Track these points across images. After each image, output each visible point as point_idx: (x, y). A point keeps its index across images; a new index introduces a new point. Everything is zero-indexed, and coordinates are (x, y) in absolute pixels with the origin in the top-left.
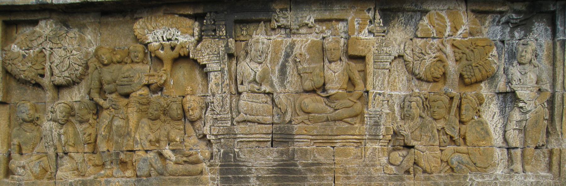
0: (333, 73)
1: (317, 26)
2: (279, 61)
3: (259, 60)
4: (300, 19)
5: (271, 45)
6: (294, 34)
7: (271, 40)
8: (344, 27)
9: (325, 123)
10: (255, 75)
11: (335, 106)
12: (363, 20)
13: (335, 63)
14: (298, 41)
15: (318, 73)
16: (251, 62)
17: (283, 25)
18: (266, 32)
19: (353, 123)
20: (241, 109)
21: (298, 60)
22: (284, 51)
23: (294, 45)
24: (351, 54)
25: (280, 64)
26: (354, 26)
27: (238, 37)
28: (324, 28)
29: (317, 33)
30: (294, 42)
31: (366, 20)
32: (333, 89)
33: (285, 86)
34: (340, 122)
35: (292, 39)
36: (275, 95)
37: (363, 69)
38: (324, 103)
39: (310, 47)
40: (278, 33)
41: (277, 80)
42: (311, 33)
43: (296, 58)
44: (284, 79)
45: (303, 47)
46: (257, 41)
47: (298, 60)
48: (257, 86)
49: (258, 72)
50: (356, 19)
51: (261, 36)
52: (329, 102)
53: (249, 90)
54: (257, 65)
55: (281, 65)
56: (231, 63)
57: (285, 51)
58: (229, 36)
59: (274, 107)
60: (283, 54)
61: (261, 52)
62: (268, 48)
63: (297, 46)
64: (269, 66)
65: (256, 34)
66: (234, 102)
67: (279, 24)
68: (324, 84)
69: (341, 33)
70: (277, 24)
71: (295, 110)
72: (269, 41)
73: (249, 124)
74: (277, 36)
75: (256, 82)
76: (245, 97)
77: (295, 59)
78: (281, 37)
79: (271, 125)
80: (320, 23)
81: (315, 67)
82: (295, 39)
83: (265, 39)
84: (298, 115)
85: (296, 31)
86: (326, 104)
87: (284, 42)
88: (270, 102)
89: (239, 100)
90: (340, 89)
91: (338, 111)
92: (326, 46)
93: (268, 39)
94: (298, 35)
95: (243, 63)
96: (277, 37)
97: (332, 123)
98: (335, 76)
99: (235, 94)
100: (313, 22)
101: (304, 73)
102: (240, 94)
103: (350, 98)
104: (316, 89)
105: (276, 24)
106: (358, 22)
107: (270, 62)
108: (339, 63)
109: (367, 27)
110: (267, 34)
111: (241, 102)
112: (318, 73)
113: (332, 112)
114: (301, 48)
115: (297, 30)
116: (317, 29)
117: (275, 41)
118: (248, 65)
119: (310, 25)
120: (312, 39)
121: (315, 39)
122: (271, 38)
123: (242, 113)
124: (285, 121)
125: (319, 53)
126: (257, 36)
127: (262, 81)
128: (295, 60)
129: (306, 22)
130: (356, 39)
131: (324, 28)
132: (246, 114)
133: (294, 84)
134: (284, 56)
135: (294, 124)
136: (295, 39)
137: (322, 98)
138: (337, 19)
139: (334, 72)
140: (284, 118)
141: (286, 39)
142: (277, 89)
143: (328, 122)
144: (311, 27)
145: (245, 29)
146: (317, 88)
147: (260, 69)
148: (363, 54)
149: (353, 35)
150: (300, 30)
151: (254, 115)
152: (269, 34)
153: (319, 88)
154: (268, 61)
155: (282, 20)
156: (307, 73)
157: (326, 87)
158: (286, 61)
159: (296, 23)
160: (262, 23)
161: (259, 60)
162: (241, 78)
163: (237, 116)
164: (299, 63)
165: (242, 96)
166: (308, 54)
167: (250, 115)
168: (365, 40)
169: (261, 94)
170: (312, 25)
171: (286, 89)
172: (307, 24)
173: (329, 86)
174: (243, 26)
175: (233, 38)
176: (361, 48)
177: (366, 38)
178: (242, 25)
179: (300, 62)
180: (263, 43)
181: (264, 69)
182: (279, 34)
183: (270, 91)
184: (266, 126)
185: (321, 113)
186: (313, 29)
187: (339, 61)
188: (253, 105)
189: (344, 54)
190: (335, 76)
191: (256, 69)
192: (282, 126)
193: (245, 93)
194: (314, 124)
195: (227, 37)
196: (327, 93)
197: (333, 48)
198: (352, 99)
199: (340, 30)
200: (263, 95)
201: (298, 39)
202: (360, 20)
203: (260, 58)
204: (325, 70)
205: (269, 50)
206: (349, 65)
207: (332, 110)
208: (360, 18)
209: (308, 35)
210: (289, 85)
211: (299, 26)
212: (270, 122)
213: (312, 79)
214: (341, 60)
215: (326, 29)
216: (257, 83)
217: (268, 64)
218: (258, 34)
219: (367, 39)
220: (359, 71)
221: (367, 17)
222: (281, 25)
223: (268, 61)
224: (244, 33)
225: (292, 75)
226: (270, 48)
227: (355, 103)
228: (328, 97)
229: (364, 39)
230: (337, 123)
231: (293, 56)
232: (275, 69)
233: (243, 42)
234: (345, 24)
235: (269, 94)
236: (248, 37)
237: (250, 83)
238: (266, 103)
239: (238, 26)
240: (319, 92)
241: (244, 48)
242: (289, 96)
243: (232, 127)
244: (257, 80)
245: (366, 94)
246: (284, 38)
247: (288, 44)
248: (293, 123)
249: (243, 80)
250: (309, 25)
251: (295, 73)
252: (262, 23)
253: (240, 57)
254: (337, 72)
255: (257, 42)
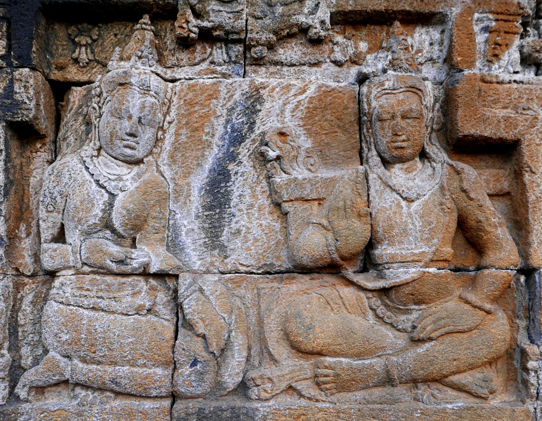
0: (404, 203)
1: (339, 38)
2: (203, 156)
3: (129, 151)
4: (280, 10)
5: (175, 99)
6: (258, 62)
7: (177, 83)
8: (431, 44)
9: (377, 392)
10: (111, 205)
11: (414, 327)
12: (501, 17)
13: (406, 166)
14: (273, 89)
15: (349, 203)
16: (101, 157)
17: (220, 27)
18: (160, 54)
19: (486, 391)
20: (50, 340)
21: (272, 154)
22: (222, 120)
23: (259, 100)
24: (466, 133)
25: (207, 166)
26: (471, 35)
27: (61, 68)
28: (363, 46)
29: (338, 64)
30: (257, 90)
31: (511, 18)
32: (404, 262)
33: (223, 248)
34: (434, 386)
35: (252, 82)
36: (185, 280)
37: (505, 185)
38: (370, 314)
39: (315, 109)
40: (204, 60)
41: (196, 225)
42: (317, 64)
43: (266, 145)
44: (221, 218)
45: (289, 107)
46: (123, 81)
47: (272, 154)
48: (114, 249)
49: (121, 196)
50: (476, 15)
51: (139, 64)
52: (386, 306)
53: (84, 264)
54: (123, 170)
55: (210, 171)
56: (29, 161)
57: (227, 121)
58: (18, 58)
59: (181, 331)
60: (220, 130)
61: (135, 118)
62: (165, 108)
63: (267, 105)
64: (168, 174)
65: (121, 59)
66: (26, 306)
67: (206, 24)
68: (371, 245)
69: (421, 64)
70: (199, 21)
71: (263, 341)
72: (171, 85)
73: (81, 392)
74: (198, 68)
75: (114, 231)
76: (69, 290)
77: (264, 148)
78: (213, 72)
79: (167, 403)
80: (349, 31)
81: (333, 181)
82: (259, 80)
83: (154, 76)
84: (275, 361)
85: (265, 52)
86: (377, 316)
87: (223, 89)
88: (166, 312)
89: (45, 300)
90: (432, 261)
91: (427, 345)
92: (374, 104)
93: (166, 80)
94: (272, 69)
95: (68, 158)
96: (199, 73)
97: (400, 391)
98: (410, 215)
99: (33, 276)
100: (328, 21)
101: (297, 199)
102: (52, 274)
103: (471, 297)
104: (342, 262)
105: (194, 21)
106: (486, 23)
107: (172, 156)
108: (419, 165)
109: (517, 42)
110: (160, 61)
111: (52, 307)
112: (349, 203)
113: (403, 350)
114: (282, 111)
115: (271, 47)
116: (337, 49)
117: (190, 87)
118: (87, 168)
119: (317, 30)
120: (320, 82)
121: (333, 84)
122: (178, 77)
123: (52, 353)
124: (218, 385)
125: (345, 130)
126: (122, 63)
127: (137, 228)
128: (262, 154)
129: (302, 19)
130: (483, 80)
131: (363, 46)
132: (68, 357)
133: (256, 240)
134: (222, 138)
135: (259, 399)
136: (261, 80)
137: (362, 294)
138: (408, 13)
139: (405, 199)
140: (217, 373)
141: (230, 81)
142: (195, 259)
143: (388, 390)
144: (317, 42)
145: (84, 40)
146: (343, 258)
147: (131, 186)
148: (509, 135)
149: (469, 68)
150: (281, 51)
151: (99, 363)
152: (171, 60)
153: (348, 259)
154: (165, 155)
155: (216, 8)
156: (307, 200)
157: (377, 252)
158: (232, 157)
159: (268, 21)
160: (146, 19)
161: (129, 151)
162: (57, 217)
163: (36, 362)
164: (276, 164)
165: (57, 283)
166: (309, 133)
167: (84, 360)
168: (515, 86)
169: (130, 279)
170: (323, 33)
171: (226, 257)
172: (304, 30)
173: (390, 250)
174: (80, 33)
175: (33, 69)
176: (501, 113)
177: (517, 77)
178: (73, 28)
179: (278, 158)
180: (146, 90)
181: (146, 183)
182: (208, 61)
183: (165, 267)
184: (148, 404)
185: (359, 356)
186: (326, 47)
187: (417, 159)
188: (97, 324)
189: (434, 135)
190: (410, 215)
191: (113, 184)
192: (211, 405)
193: (71, 272)
194: (334, 398)
195: (10, 65)
196: (381, 276)
197: (399, 110)
198: (479, 303)
199: (417, 53)
200: (142, 284)
201: (273, 82)
202: (491, 16)
203: (131, 142)
204: (372, 192)
205: (168, 118)
206: (458, 173)
207: (401, 340)
208: (491, 12)
209: (305, 68)
210: (238, 242)
211: (275, 33)
212: (164, 391)
213: (325, 222)
214: (423, 155)
215: (370, 50)
216: (118, 238)
217: (163, 168)
218: (129, 58)
219: (522, 82)
220: (490, 195)
221: (513, 10)
222: (214, 28)
223: (165, 155)
224: (84, 55)
225: (252, 206)
226: (173, 114)
227: (488, 313)
228: (384, 292)
229: (510, 82)
230: (423, 391)
231: (254, 140)
232: (188, 184)
233: (79, 88)
234: (435, 34)
235: (161, 276)
236: (97, 68)
237: (87, 234)
238: (149, 311)
239: (60, 31)
240: (350, 272)
241: (80, 107)
242: (238, 284)
243: (11, 409)
244: (117, 224)
245: (522, 279)
246: (224, 76)
247: (237, 96)
248: (254, 392)
249: (65, 222)
250: (312, 33)
251: (264, 201)
252: (146, 19)
253: (65, 139)
254: (418, 199)
255: (121, 84)
